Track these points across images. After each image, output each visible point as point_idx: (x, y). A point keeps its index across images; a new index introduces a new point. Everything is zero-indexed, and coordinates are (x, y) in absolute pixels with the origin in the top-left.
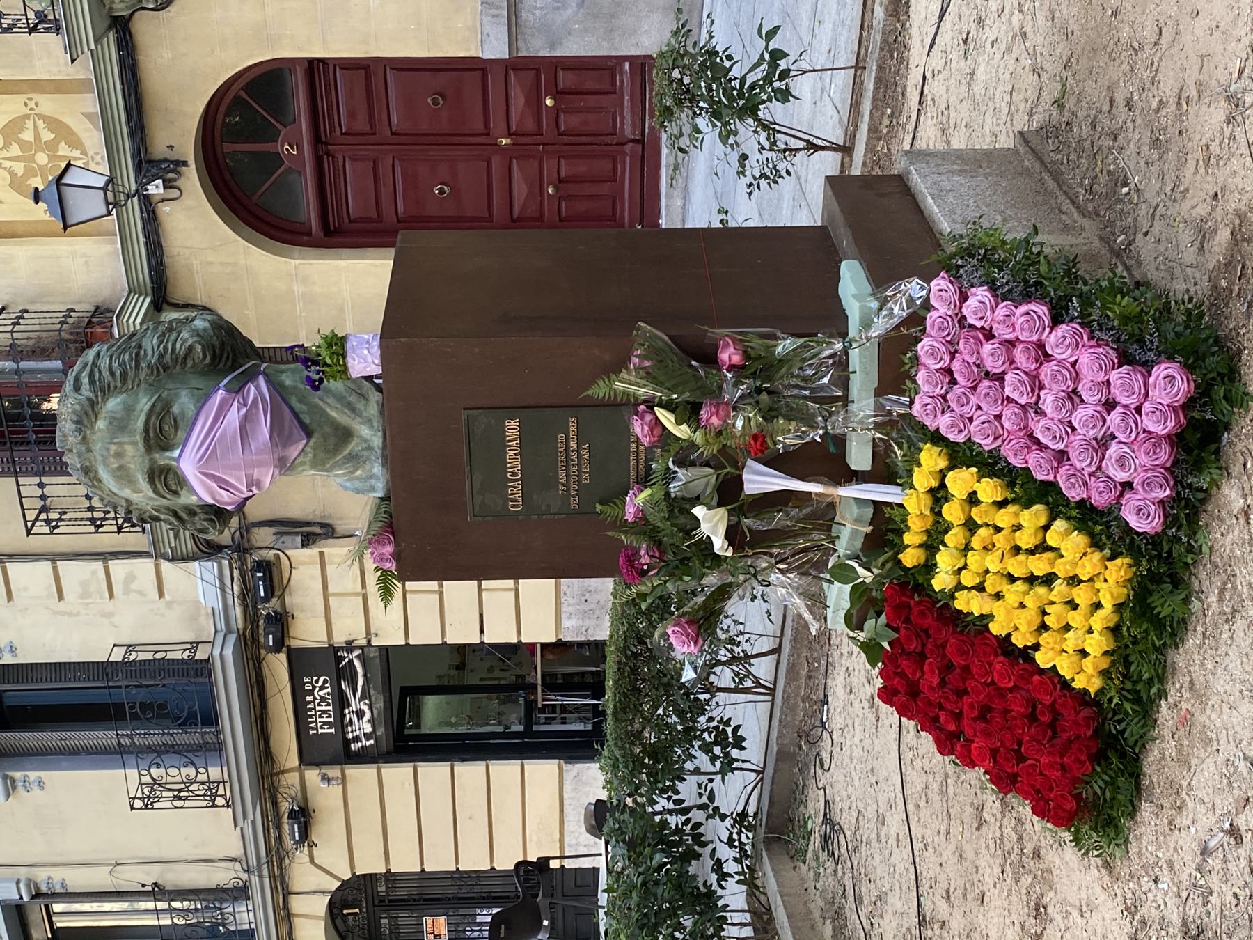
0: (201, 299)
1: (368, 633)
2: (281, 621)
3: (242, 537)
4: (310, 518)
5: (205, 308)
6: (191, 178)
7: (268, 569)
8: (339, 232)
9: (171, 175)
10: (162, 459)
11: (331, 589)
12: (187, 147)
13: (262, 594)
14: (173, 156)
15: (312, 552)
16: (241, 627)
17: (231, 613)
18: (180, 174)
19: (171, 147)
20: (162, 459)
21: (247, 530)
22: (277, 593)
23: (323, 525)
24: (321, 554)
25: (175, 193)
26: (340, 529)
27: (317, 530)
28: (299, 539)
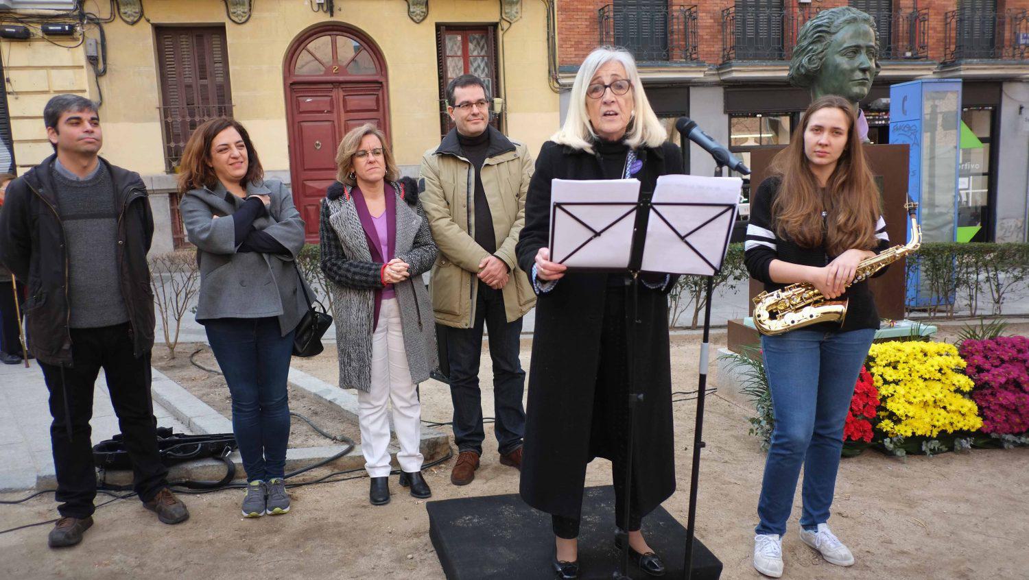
0: (255, 14)
1: (17, 93)
2: (23, 37)
3: (92, 19)
4: (109, 61)
5: (250, 16)
6: (324, 18)
7: (69, 34)
8: (292, 90)
9: (325, 8)
10: (864, 51)
11: (54, 72)
12: (339, 18)
13: (51, 28)
14: (335, 9)
15: (83, 61)
16: (18, 11)
17: (33, 6)
18: (325, 12)
19: (340, 10)
20: (864, 51)
21: (98, 24)
22: (46, 37)
23: (105, 71)
24: (82, 67)
25: (316, 8)
26: (104, 81)
27: (101, 67)
28: (94, 54)
